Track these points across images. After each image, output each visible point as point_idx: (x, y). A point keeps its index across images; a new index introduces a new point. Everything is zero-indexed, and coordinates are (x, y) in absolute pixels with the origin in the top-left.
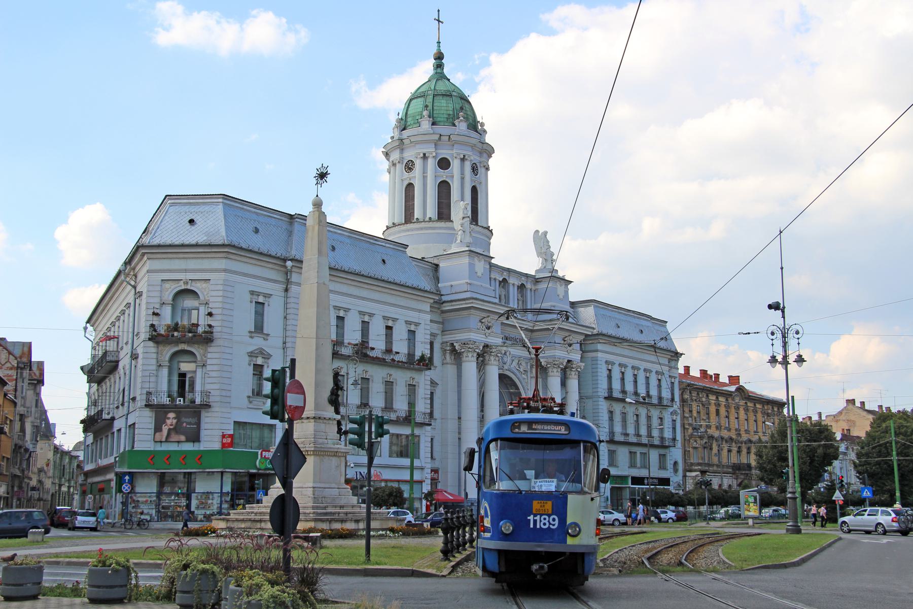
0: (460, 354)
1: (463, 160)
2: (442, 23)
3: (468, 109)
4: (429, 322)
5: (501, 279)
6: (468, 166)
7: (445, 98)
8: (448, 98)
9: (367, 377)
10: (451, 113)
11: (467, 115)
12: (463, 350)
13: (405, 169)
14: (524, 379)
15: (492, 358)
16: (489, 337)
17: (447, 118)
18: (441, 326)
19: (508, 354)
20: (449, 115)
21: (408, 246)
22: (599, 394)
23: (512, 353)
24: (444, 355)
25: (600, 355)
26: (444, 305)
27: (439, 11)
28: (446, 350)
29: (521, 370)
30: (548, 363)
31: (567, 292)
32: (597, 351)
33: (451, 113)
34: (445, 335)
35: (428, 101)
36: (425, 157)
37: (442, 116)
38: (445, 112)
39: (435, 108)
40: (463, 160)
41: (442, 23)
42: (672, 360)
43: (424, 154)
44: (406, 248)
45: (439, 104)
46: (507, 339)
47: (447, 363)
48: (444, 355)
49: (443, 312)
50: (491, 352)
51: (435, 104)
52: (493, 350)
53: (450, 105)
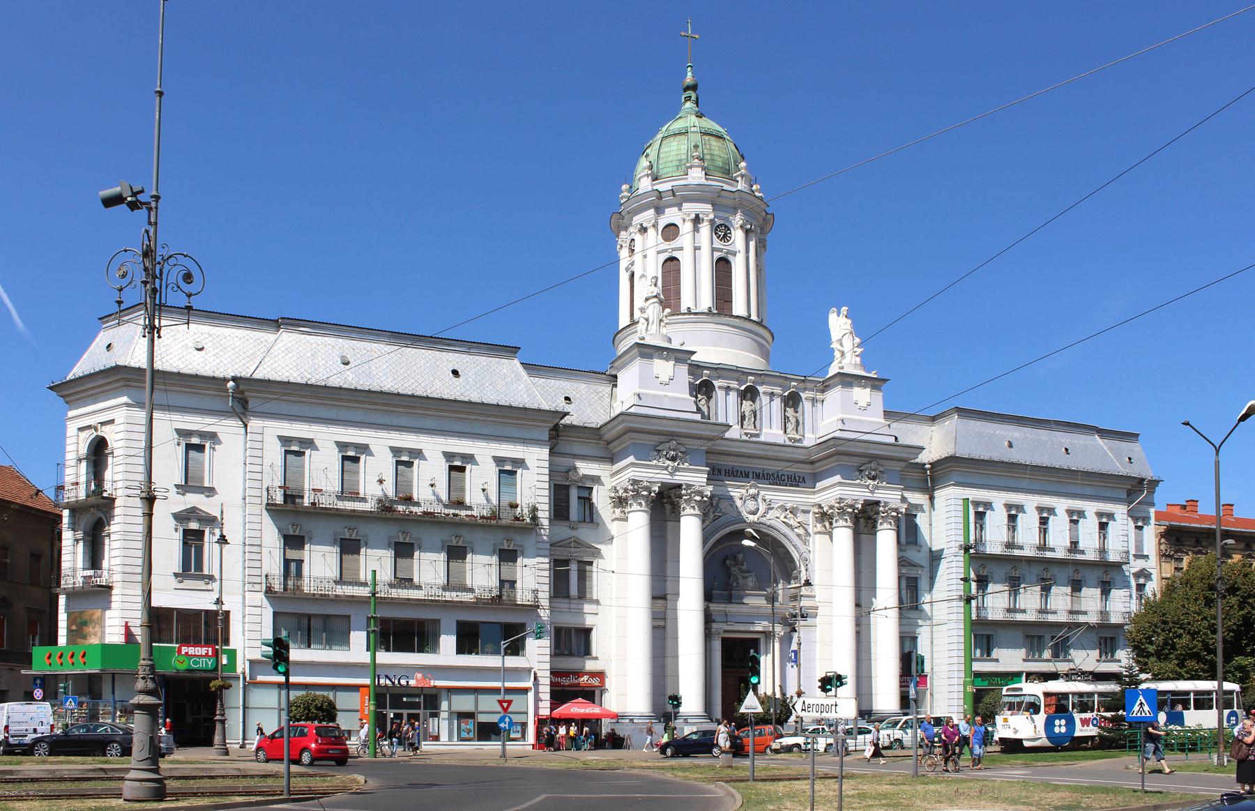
1: (697, 220)
3: (713, 148)
6: (705, 229)
7: (678, 138)
8: (683, 137)
14: (799, 535)
20: (681, 160)
23: (767, 497)
33: (684, 157)
38: (675, 158)
39: (661, 156)
40: (697, 220)
42: (1135, 491)
43: (641, 225)
45: (667, 149)
51: (661, 151)
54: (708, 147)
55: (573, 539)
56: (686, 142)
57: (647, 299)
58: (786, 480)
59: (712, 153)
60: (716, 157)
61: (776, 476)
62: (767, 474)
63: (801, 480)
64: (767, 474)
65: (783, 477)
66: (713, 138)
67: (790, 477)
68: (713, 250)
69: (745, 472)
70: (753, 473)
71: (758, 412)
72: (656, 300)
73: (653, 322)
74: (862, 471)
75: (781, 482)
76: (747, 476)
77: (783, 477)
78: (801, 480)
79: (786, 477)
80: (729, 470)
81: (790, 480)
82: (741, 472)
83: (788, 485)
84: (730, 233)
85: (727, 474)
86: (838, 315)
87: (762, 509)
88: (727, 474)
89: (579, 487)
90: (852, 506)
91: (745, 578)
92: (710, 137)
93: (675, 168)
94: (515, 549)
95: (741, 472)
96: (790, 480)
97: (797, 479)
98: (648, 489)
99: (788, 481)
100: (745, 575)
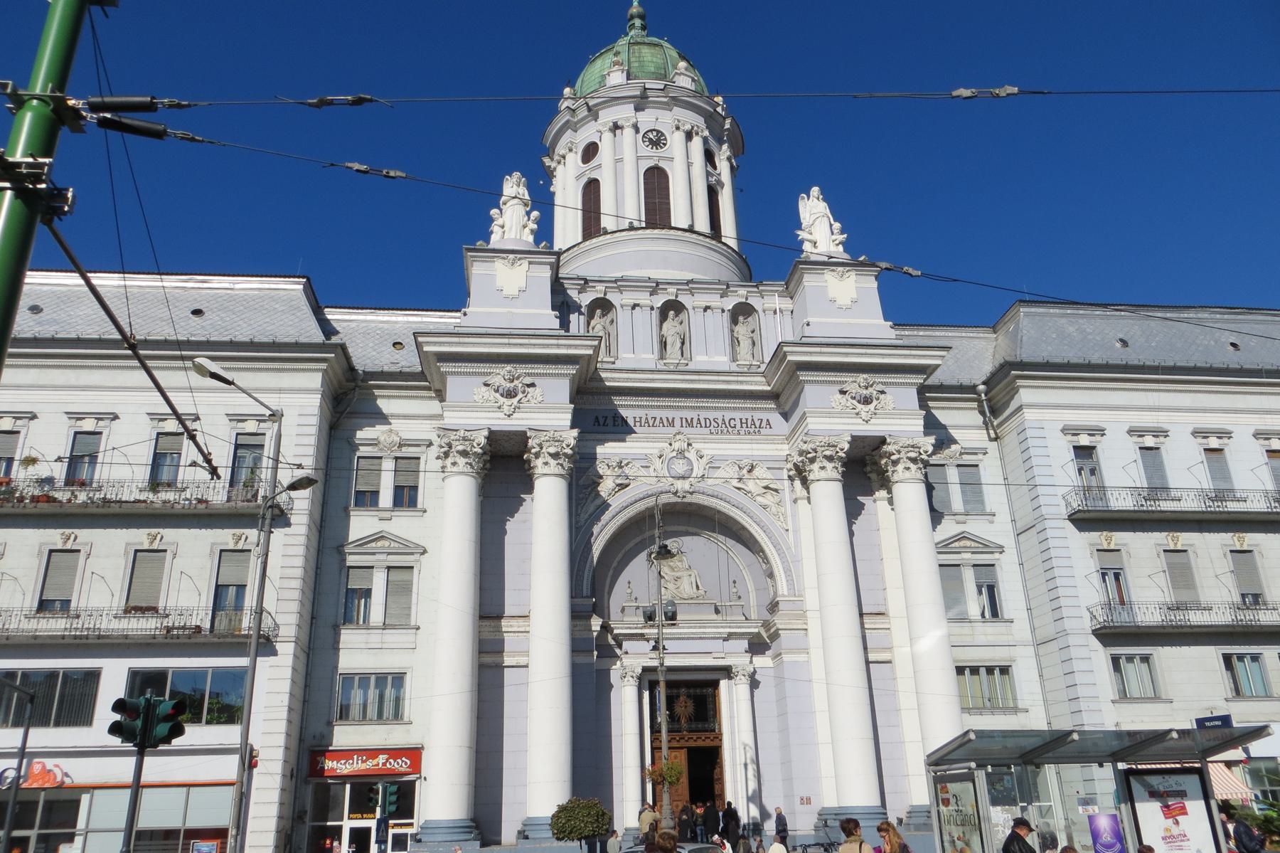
23: (705, 452)
54: (637, 55)
59: (641, 59)
60: (646, 64)
61: (720, 422)
62: (705, 419)
63: (764, 424)
64: (705, 419)
65: (732, 421)
66: (646, 47)
67: (744, 421)
68: (638, 158)
69: (667, 418)
70: (681, 418)
71: (687, 335)
72: (516, 201)
73: (511, 228)
75: (730, 429)
77: (732, 421)
78: (764, 424)
81: (744, 425)
82: (661, 419)
83: (742, 432)
84: (665, 139)
87: (697, 471)
92: (641, 47)
95: (661, 419)
96: (744, 425)
97: (757, 424)
99: (742, 427)
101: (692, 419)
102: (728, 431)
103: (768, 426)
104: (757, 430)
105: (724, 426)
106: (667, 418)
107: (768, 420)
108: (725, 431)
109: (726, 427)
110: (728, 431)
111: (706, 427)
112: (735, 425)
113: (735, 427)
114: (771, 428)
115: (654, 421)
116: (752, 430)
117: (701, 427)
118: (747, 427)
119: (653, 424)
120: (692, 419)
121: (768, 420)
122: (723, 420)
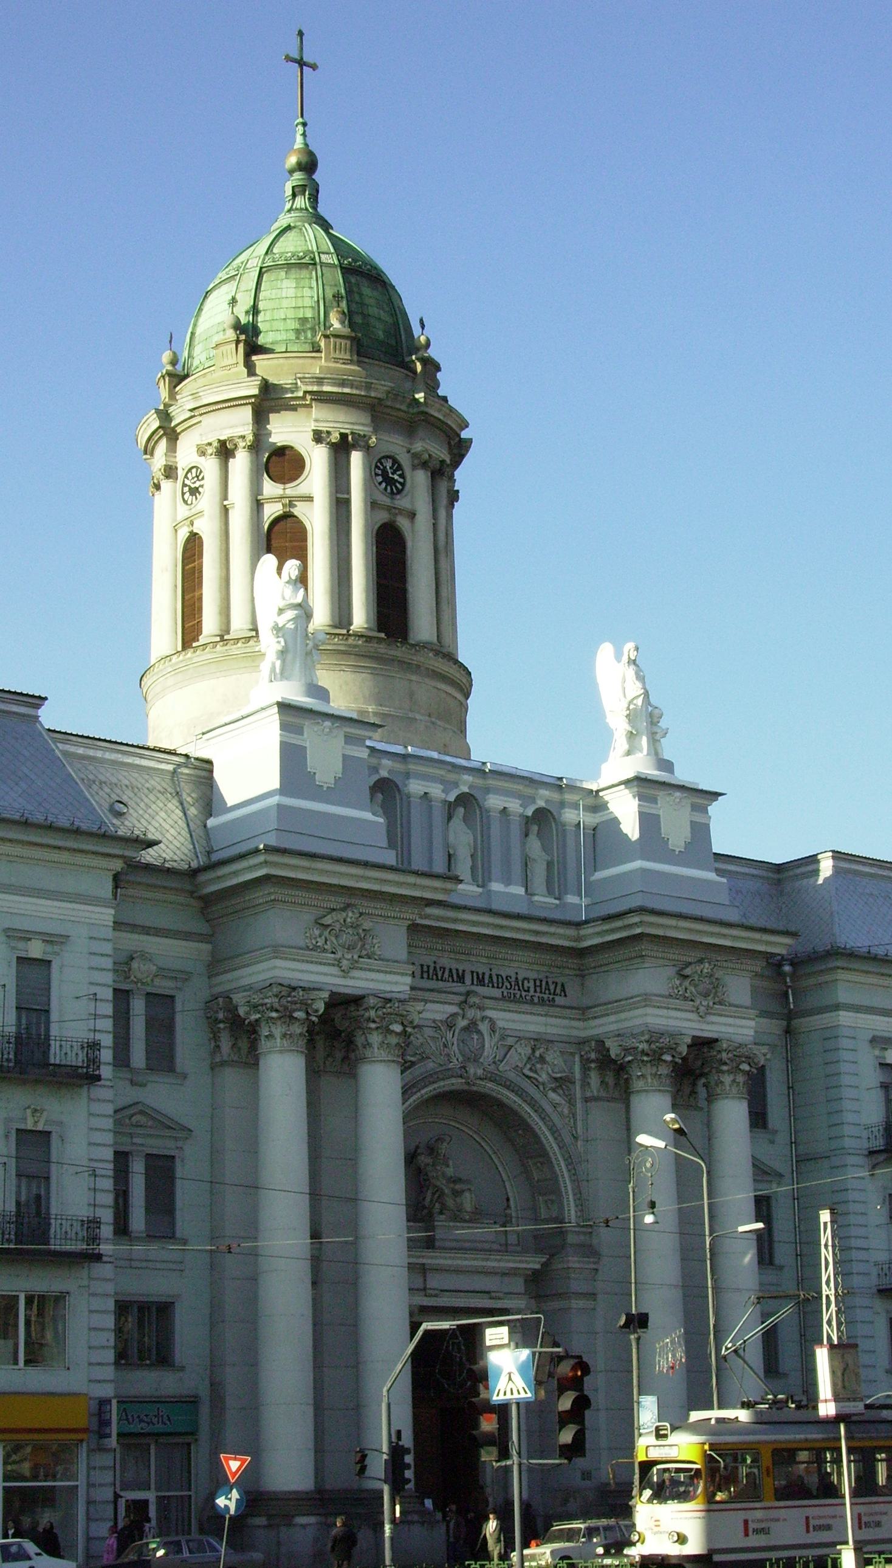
0: (252, 1030)
2: (314, 67)
3: (367, 301)
4: (110, 933)
5: (452, 798)
7: (294, 274)
8: (304, 273)
9: (40, 1127)
10: (309, 314)
11: (365, 316)
12: (255, 1017)
13: (183, 494)
14: (555, 1106)
15: (375, 1038)
16: (356, 973)
17: (298, 332)
18: (206, 947)
19: (484, 1027)
21: (46, 699)
22: (848, 1142)
23: (500, 1024)
24: (215, 1037)
25: (845, 1018)
26: (203, 877)
27: (301, 34)
28: (217, 1021)
29: (543, 1077)
30: (627, 1050)
31: (701, 832)
32: (837, 1007)
34: (217, 974)
35: (243, 287)
36: (225, 451)
37: (281, 325)
38: (291, 314)
41: (314, 67)
44: (38, 706)
45: (274, 294)
46: (481, 982)
47: (223, 1064)
48: (215, 1037)
49: (207, 902)
50: (369, 1020)
51: (262, 295)
52: (372, 1013)
53: (307, 292)
54: (357, 297)
55: (140, 1107)
56: (314, 284)
57: (281, 611)
58: (532, 990)
60: (372, 321)
62: (498, 976)
63: (558, 991)
64: (498, 976)
69: (457, 970)
70: (472, 972)
74: (686, 977)
75: (524, 994)
76: (461, 979)
79: (531, 984)
80: (428, 967)
81: (538, 989)
82: (451, 970)
83: (536, 1000)
85: (425, 975)
86: (618, 657)
88: (425, 975)
89: (148, 994)
90: (671, 1049)
91: (457, 1194)
93: (292, 336)
94: (48, 1129)
95: (451, 970)
96: (538, 989)
97: (552, 987)
98: (306, 1006)
99: (535, 991)
100: (458, 1187)
101: (484, 974)
102: (521, 996)
103: (563, 994)
104: (551, 997)
105: (517, 988)
106: (457, 970)
107: (563, 985)
108: (518, 996)
109: (519, 990)
110: (521, 996)
111: (498, 987)
112: (529, 988)
113: (528, 991)
114: (565, 996)
115: (443, 973)
116: (546, 996)
117: (493, 987)
118: (541, 992)
119: (442, 976)
120: (484, 974)
121: (563, 985)
122: (517, 978)
